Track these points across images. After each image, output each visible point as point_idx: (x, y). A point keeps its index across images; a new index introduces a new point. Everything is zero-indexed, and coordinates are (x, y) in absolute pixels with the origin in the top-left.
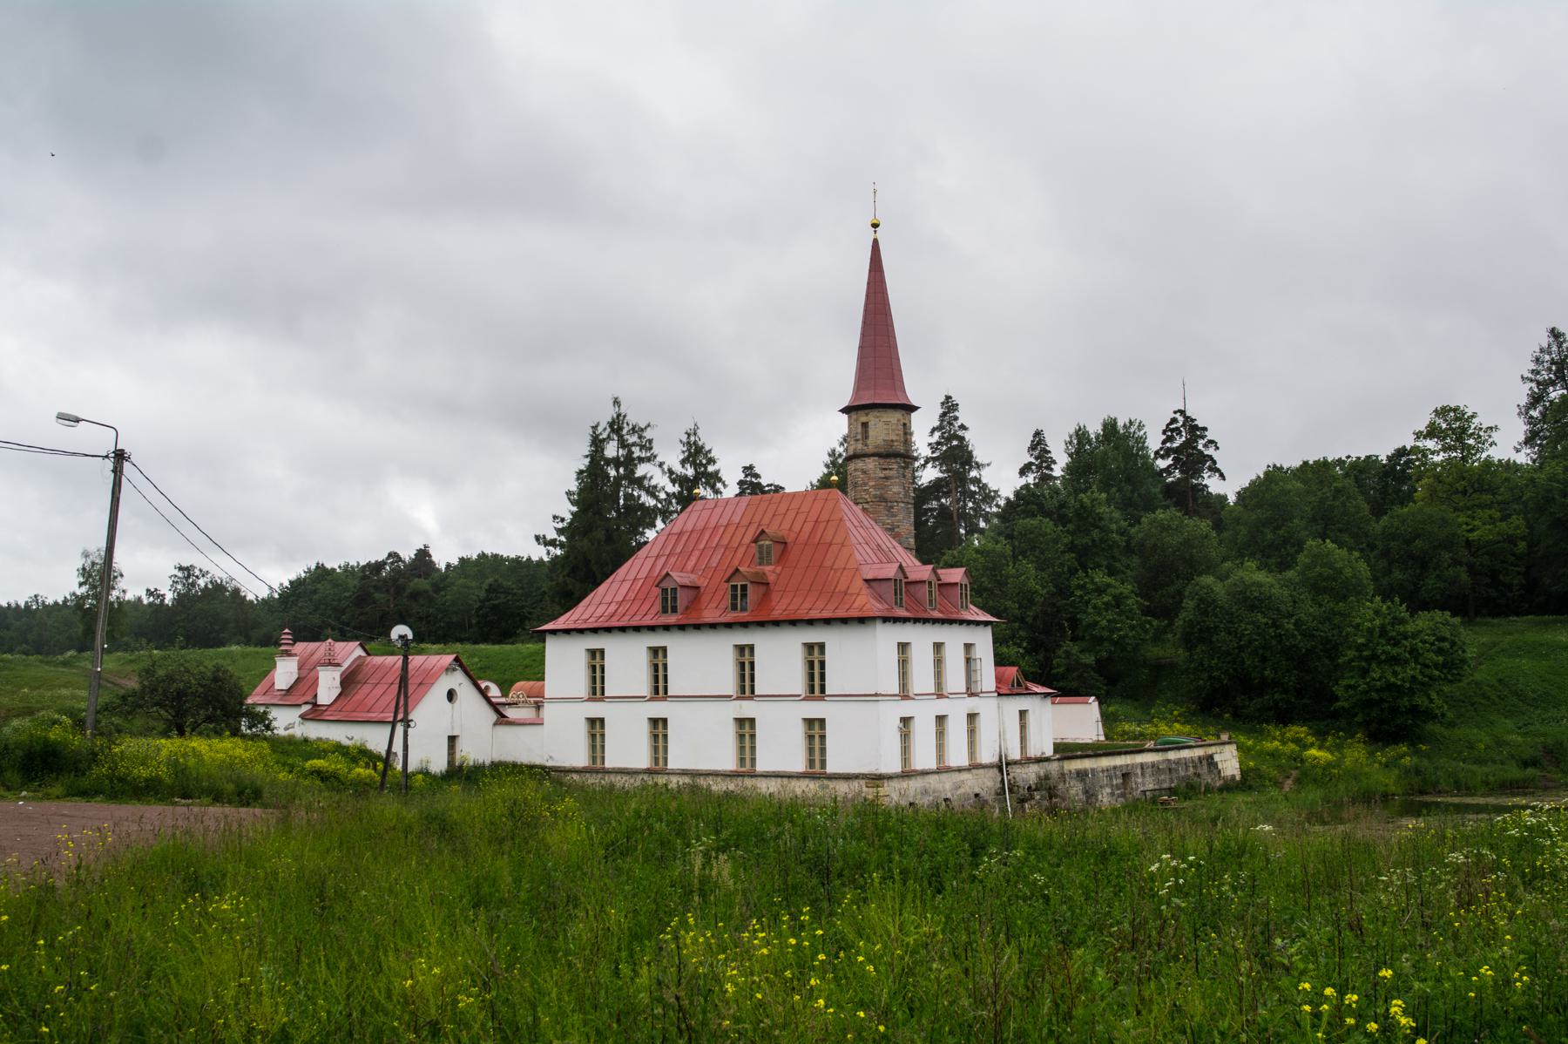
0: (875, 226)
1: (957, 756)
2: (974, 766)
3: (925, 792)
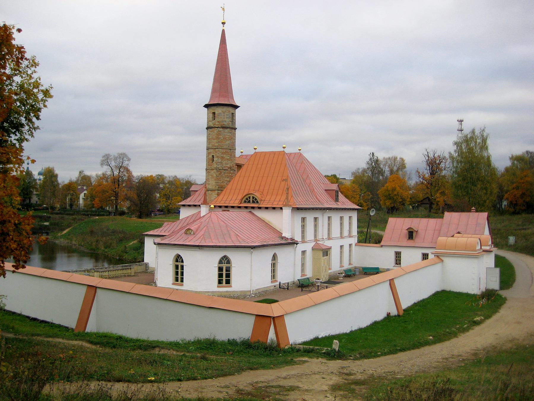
0: (223, 23)
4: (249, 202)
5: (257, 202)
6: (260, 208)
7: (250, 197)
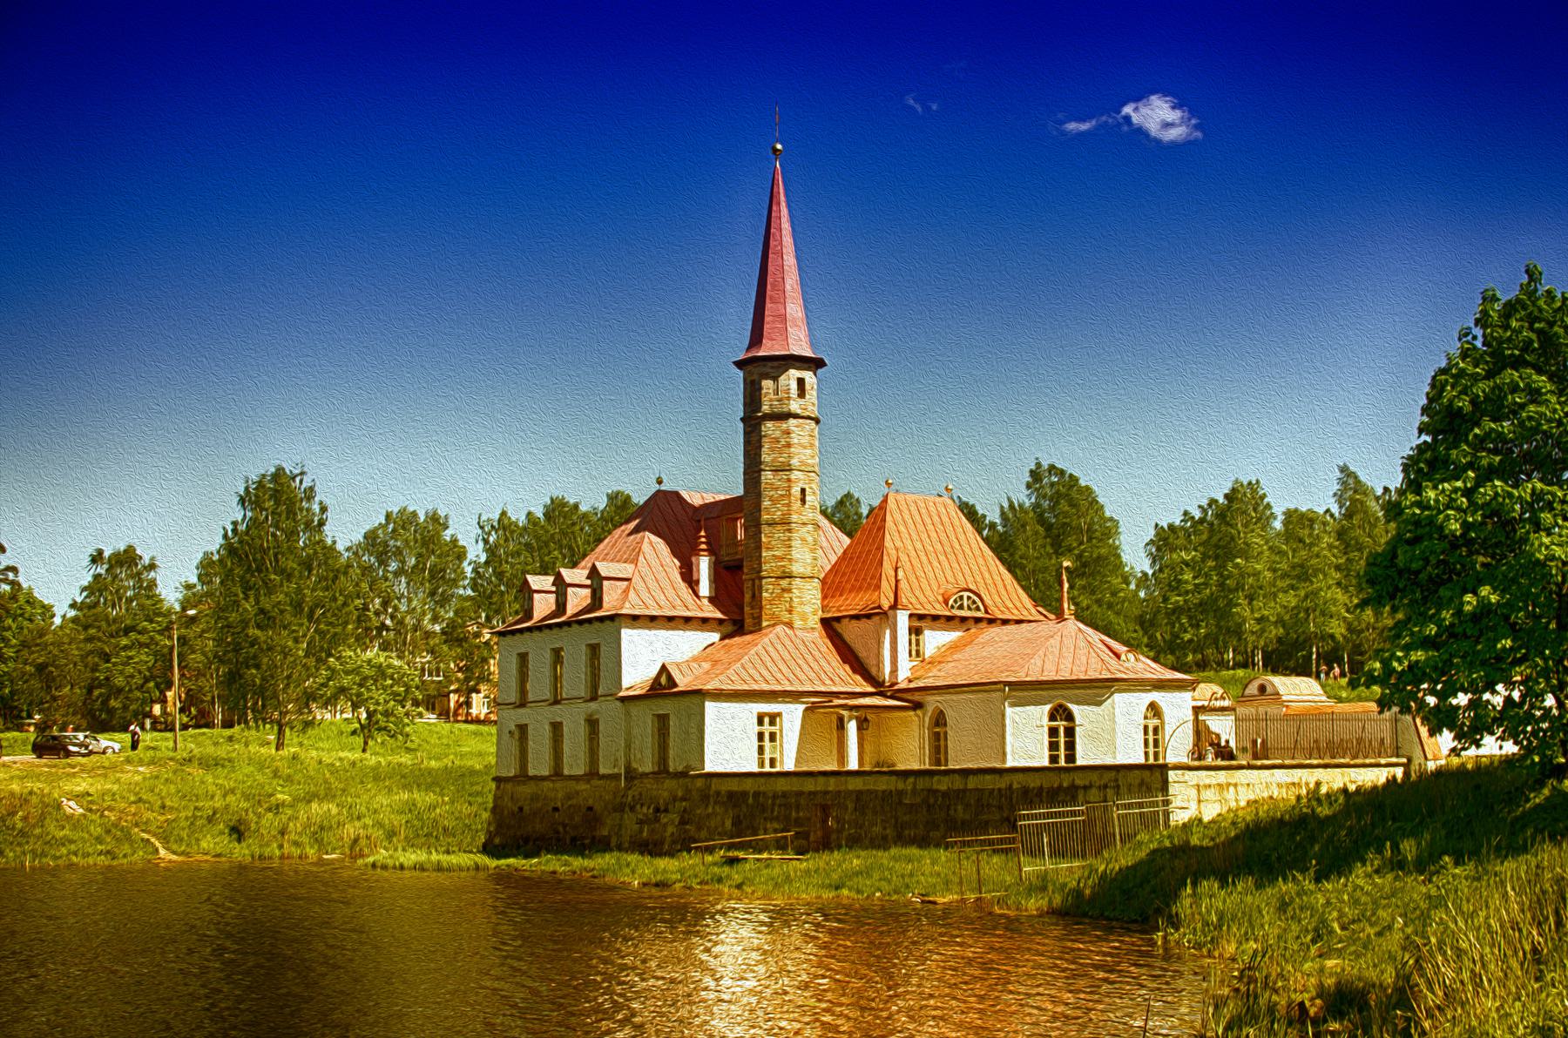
1: (575, 765)
2: (592, 774)
3: (534, 798)
4: (961, 607)
5: (978, 609)
6: (991, 621)
7: (961, 598)
